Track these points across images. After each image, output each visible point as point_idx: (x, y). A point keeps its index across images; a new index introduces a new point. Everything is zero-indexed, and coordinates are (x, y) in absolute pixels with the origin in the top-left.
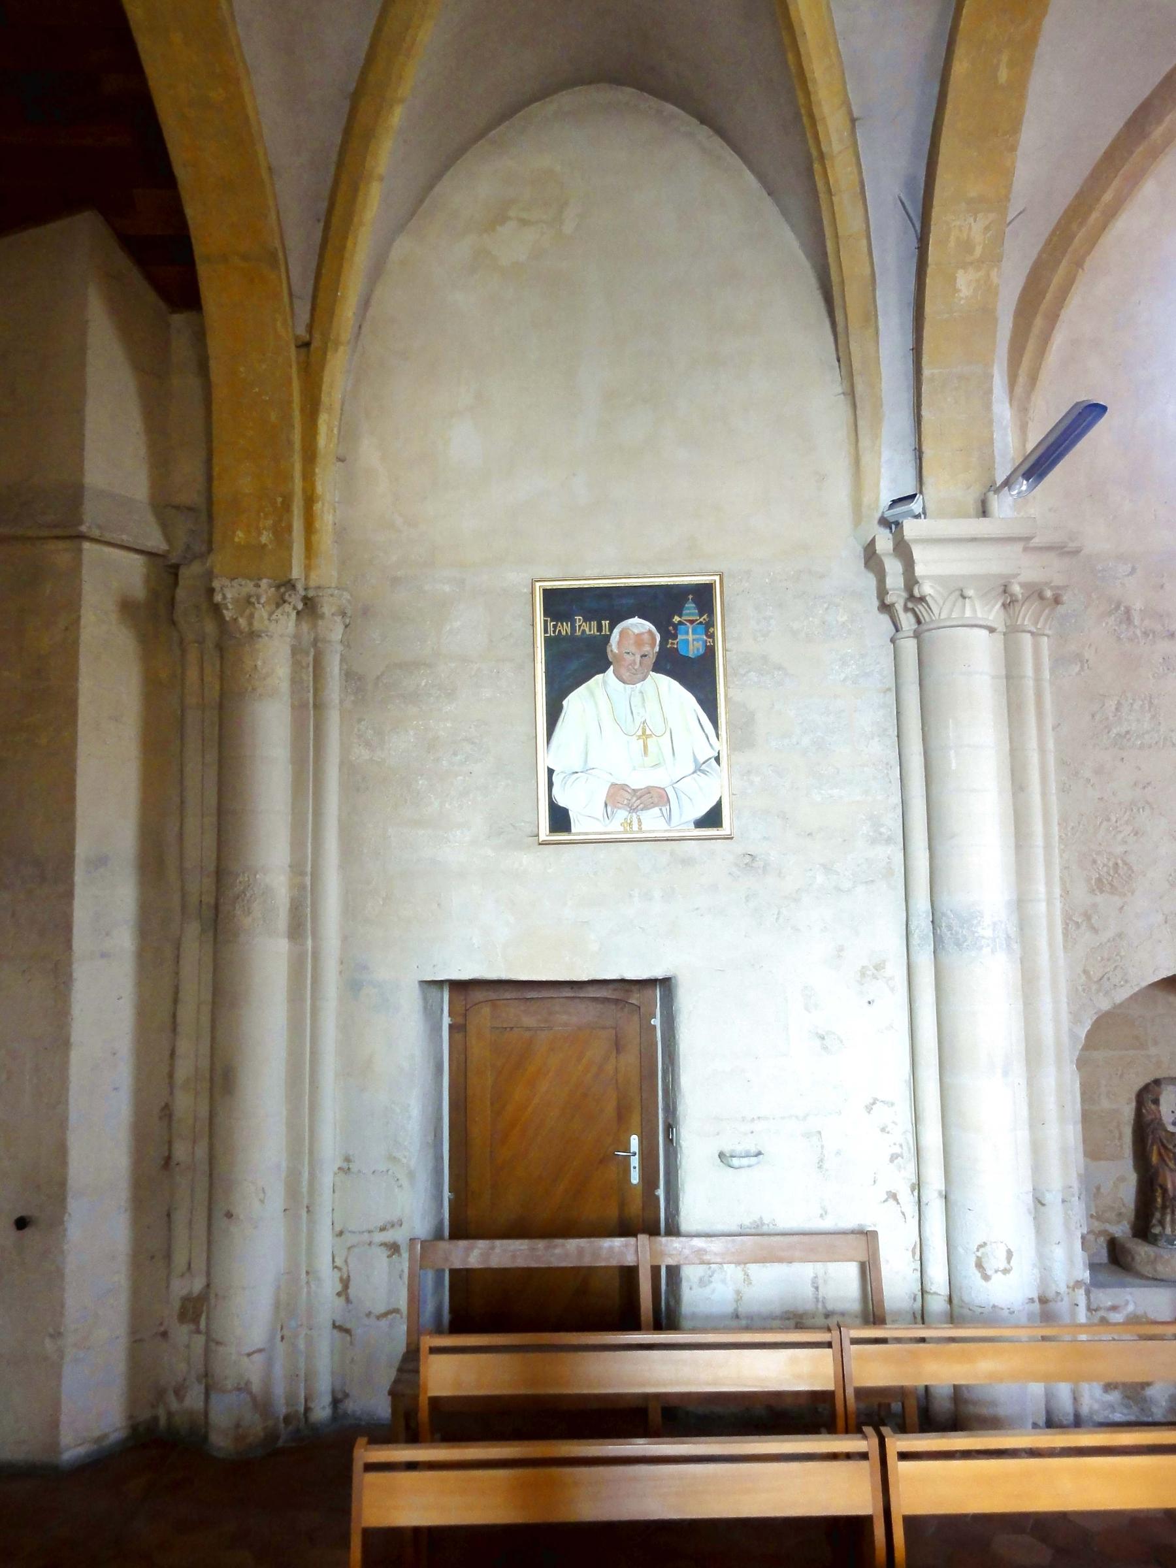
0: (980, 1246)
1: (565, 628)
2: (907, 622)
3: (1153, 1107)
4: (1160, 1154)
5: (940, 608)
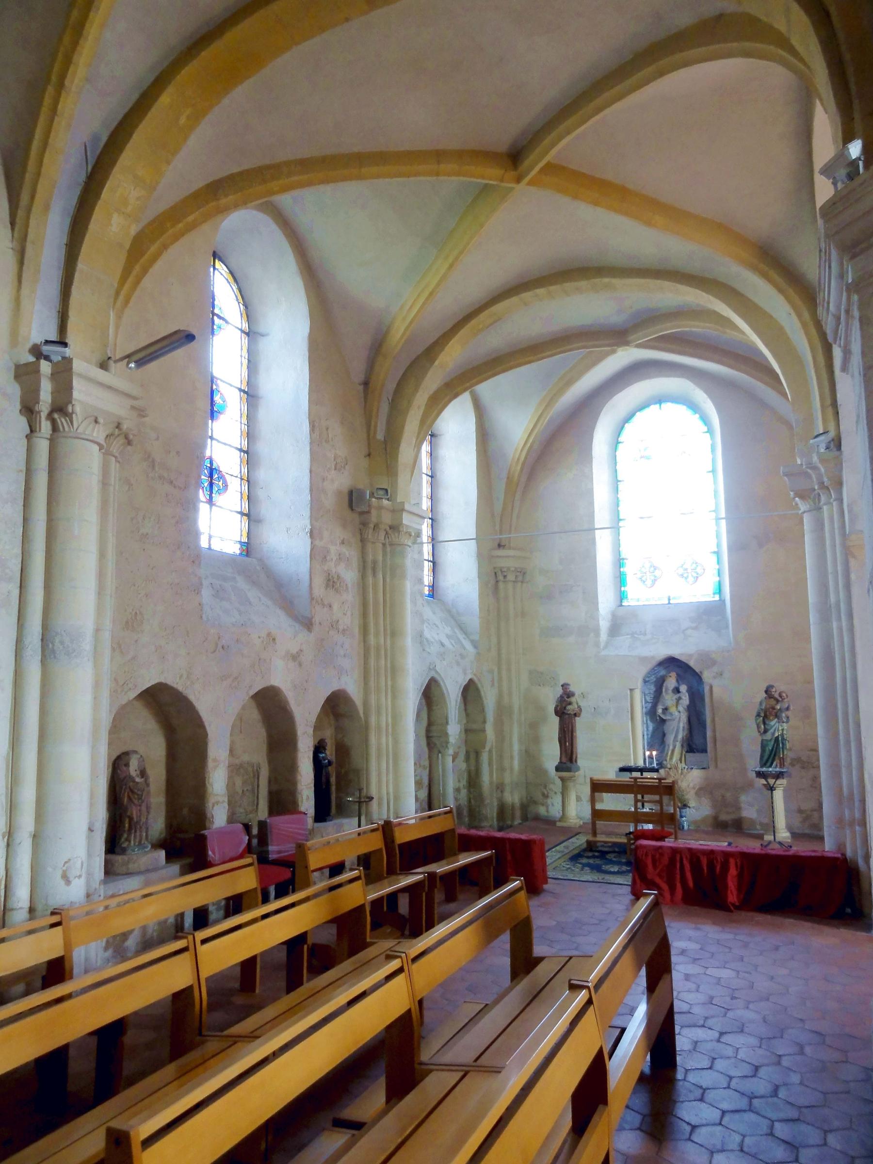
0: (66, 862)
2: (45, 427)
3: (124, 768)
4: (129, 797)
5: (80, 423)
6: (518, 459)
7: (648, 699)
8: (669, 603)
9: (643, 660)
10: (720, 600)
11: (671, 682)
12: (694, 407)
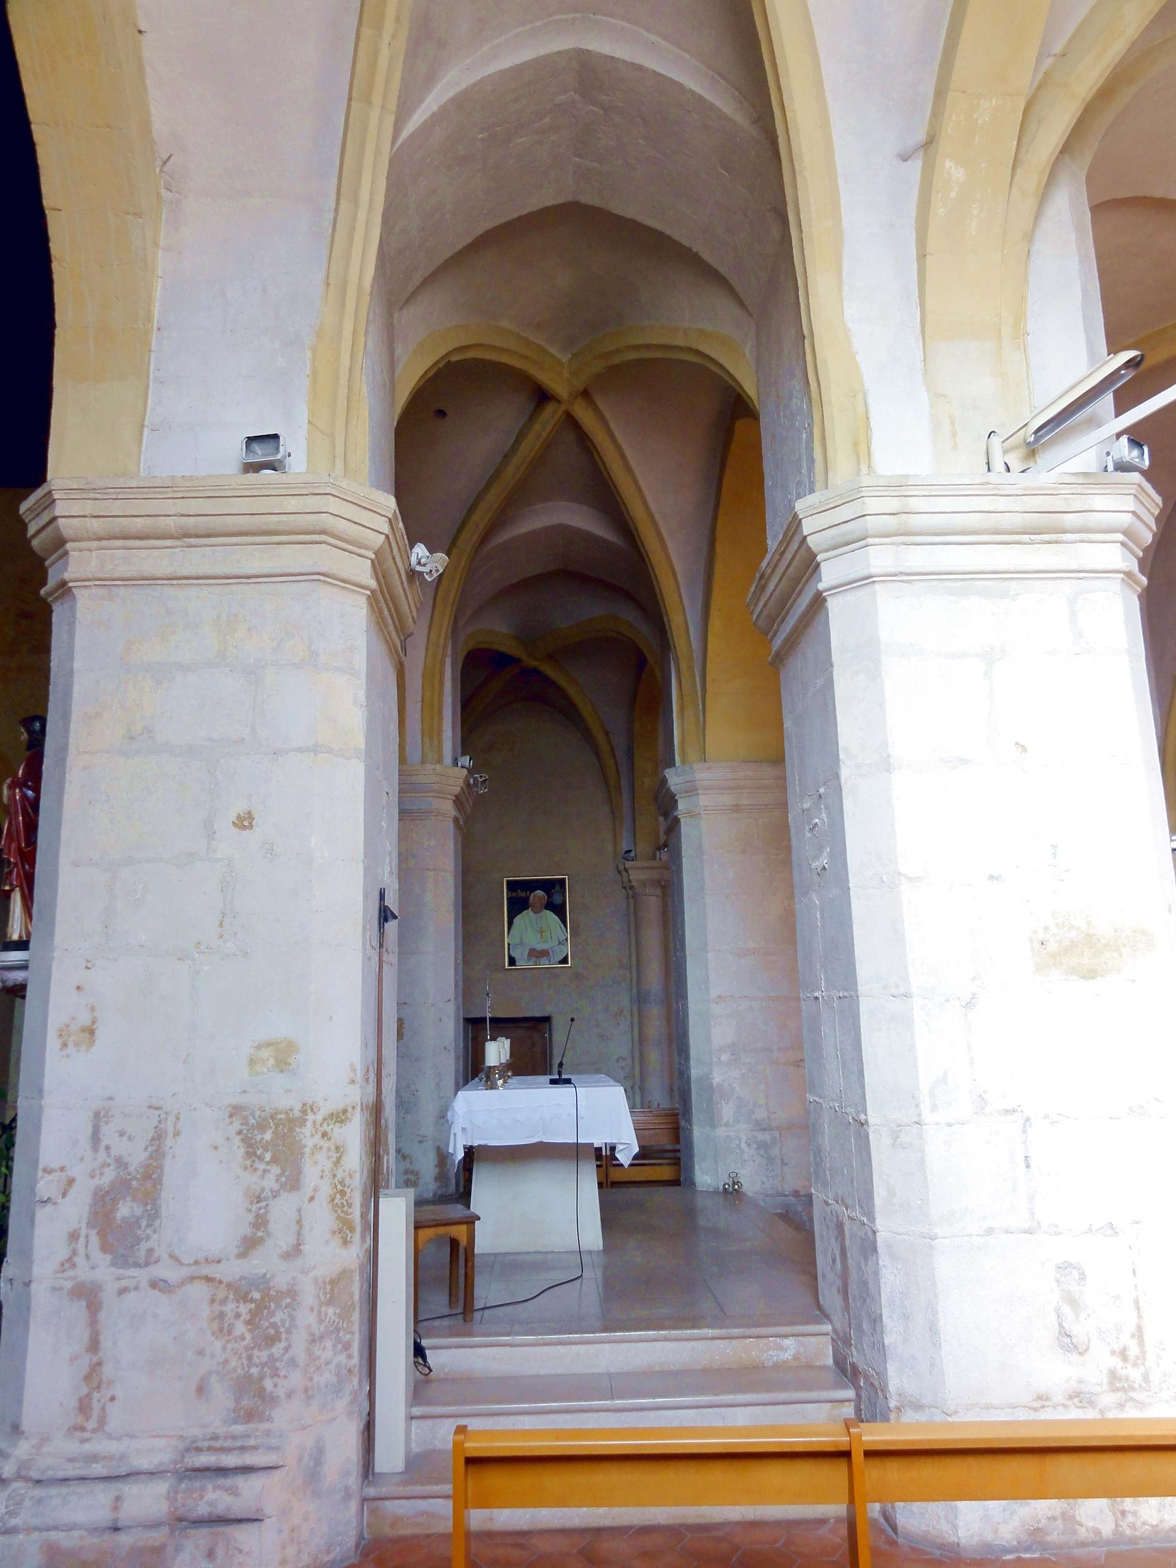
1: (514, 894)
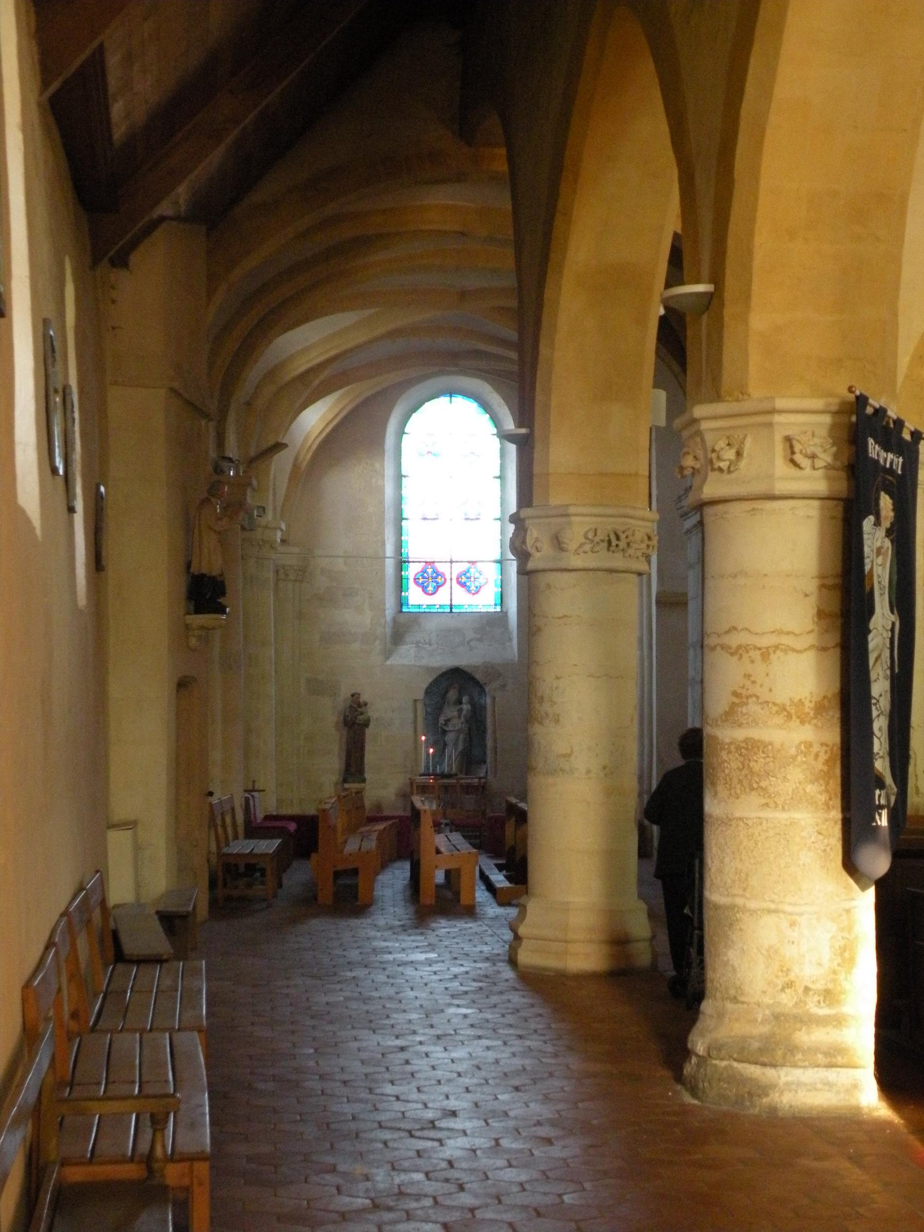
6: (310, 447)
7: (429, 710)
8: (451, 612)
9: (429, 670)
10: (502, 611)
11: (452, 695)
12: (485, 406)
